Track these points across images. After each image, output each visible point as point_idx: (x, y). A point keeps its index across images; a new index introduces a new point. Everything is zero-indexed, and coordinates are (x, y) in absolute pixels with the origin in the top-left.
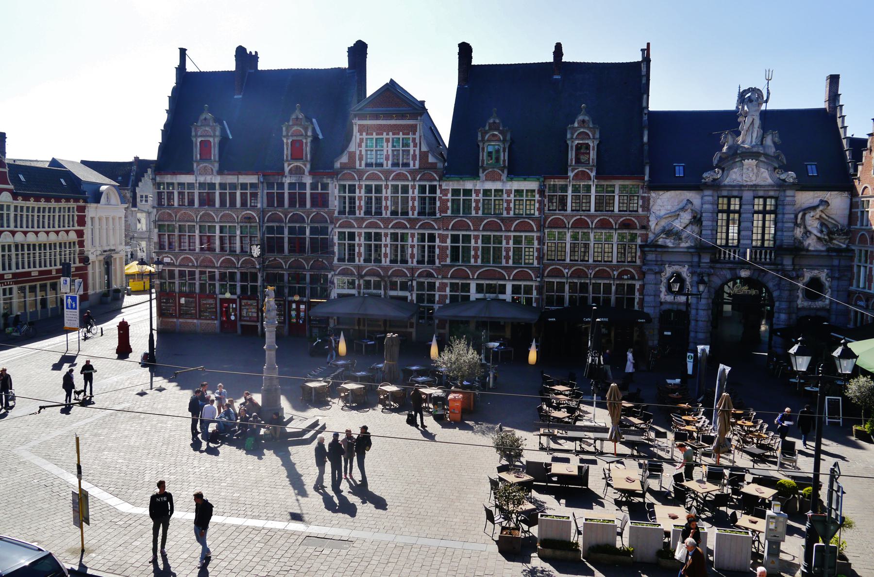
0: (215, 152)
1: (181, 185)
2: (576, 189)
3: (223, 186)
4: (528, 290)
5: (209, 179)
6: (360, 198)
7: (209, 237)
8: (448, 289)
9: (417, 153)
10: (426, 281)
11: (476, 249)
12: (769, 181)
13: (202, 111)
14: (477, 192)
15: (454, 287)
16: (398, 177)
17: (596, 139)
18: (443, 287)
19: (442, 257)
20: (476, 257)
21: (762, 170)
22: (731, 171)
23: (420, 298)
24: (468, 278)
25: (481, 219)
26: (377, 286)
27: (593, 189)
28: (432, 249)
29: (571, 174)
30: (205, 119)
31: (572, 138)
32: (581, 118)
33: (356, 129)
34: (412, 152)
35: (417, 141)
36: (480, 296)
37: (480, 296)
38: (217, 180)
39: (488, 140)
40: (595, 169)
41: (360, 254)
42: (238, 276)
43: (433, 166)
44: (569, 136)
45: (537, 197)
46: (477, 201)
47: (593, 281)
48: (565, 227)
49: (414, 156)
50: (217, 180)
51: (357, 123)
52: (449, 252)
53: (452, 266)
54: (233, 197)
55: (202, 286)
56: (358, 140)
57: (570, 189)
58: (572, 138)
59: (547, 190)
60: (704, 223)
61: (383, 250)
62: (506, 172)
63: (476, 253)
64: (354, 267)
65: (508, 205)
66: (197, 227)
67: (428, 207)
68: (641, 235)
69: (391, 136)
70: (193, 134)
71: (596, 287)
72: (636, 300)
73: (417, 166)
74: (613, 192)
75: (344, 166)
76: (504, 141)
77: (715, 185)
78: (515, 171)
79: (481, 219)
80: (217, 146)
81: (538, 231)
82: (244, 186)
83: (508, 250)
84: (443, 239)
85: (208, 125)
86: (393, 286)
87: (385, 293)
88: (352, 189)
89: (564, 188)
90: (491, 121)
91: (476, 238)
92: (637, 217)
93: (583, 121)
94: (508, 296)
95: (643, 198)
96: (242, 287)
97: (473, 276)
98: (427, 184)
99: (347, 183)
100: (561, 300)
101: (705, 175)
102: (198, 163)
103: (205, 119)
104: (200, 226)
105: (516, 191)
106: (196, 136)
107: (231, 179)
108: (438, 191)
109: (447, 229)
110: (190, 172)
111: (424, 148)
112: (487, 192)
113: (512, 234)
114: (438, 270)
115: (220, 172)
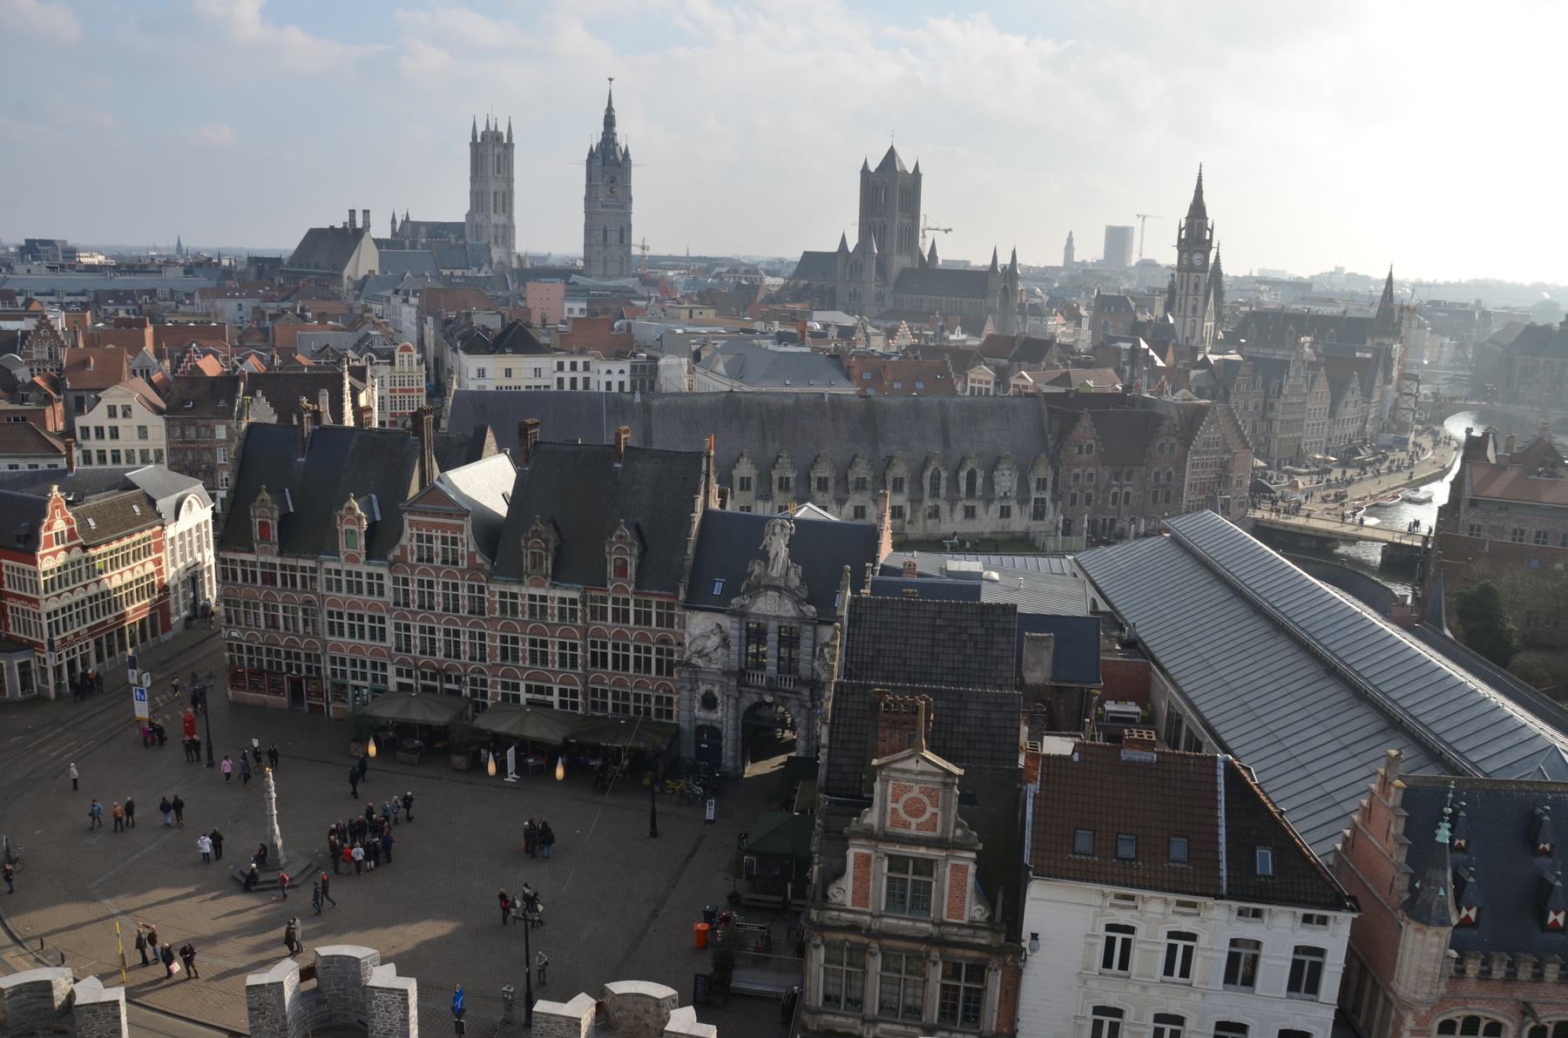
0: (274, 533)
1: (243, 562)
2: (615, 601)
3: (283, 567)
4: (574, 694)
5: (270, 559)
6: (413, 592)
7: (273, 615)
8: (499, 687)
9: (465, 552)
10: (479, 677)
11: (524, 651)
12: (792, 613)
13: (259, 491)
14: (523, 596)
15: (505, 685)
16: (448, 574)
17: (634, 555)
18: (494, 684)
19: (493, 657)
20: (524, 659)
21: (787, 601)
22: (759, 600)
23: (474, 692)
24: (517, 677)
25: (527, 623)
26: (433, 678)
27: (632, 603)
28: (483, 647)
29: (610, 587)
30: (263, 500)
31: (610, 552)
32: (618, 533)
33: (406, 524)
34: (460, 552)
35: (465, 541)
36: (530, 696)
37: (530, 696)
38: (278, 561)
39: (531, 547)
40: (633, 585)
41: (415, 646)
42: (303, 656)
43: (480, 568)
44: (607, 550)
45: (579, 606)
46: (523, 605)
47: (634, 691)
48: (606, 637)
49: (463, 555)
50: (278, 561)
51: (407, 518)
52: (498, 652)
53: (502, 666)
54: (293, 578)
55: (270, 663)
56: (409, 535)
57: (610, 601)
58: (610, 552)
59: (588, 600)
60: (732, 648)
61: (437, 643)
62: (549, 579)
63: (524, 656)
64: (411, 657)
65: (552, 612)
66: (261, 605)
67: (478, 608)
68: (677, 651)
69: (440, 534)
70: (252, 514)
71: (637, 697)
72: (675, 713)
73: (466, 566)
74: (651, 607)
75: (397, 559)
76: (547, 549)
77: (741, 614)
78: (558, 578)
79: (527, 623)
80: (276, 527)
81: (581, 639)
82: (303, 569)
83: (553, 655)
84: (493, 639)
85: (265, 506)
86: (449, 680)
87: (441, 686)
88: (405, 582)
89: (604, 600)
90: (534, 528)
91: (524, 640)
92: (675, 634)
93: (621, 537)
94: (555, 699)
95: (679, 615)
96: (307, 667)
97: (522, 675)
98: (476, 584)
99: (401, 576)
100: (605, 705)
101: (733, 601)
102: (258, 544)
103: (263, 500)
104: (264, 605)
105: (559, 598)
106: (255, 517)
107: (290, 561)
108: (486, 592)
109: (496, 630)
110: (251, 551)
111: (472, 549)
112: (532, 597)
113: (557, 640)
114: (488, 667)
115: (280, 554)
